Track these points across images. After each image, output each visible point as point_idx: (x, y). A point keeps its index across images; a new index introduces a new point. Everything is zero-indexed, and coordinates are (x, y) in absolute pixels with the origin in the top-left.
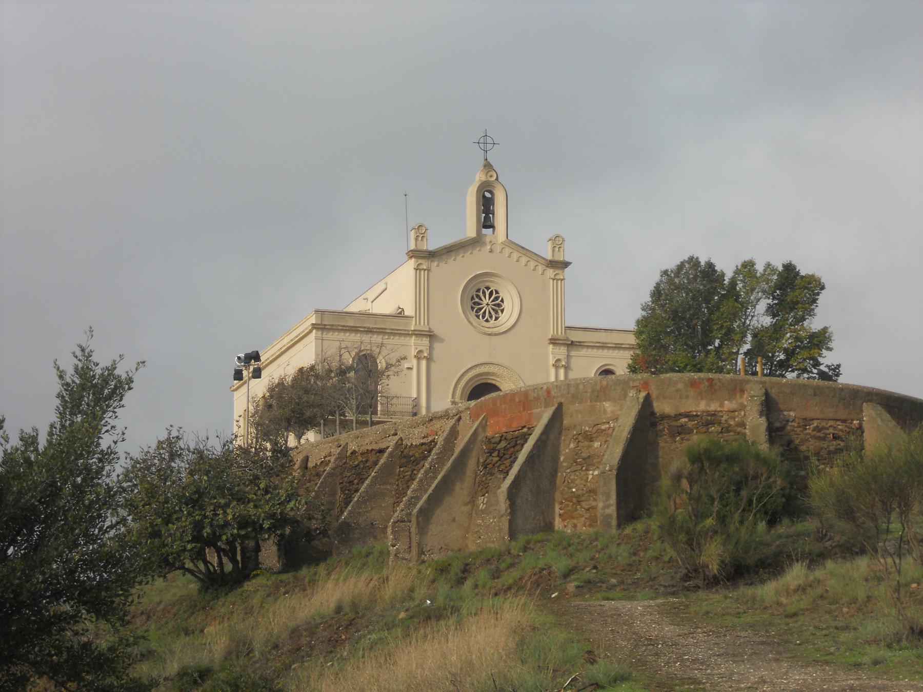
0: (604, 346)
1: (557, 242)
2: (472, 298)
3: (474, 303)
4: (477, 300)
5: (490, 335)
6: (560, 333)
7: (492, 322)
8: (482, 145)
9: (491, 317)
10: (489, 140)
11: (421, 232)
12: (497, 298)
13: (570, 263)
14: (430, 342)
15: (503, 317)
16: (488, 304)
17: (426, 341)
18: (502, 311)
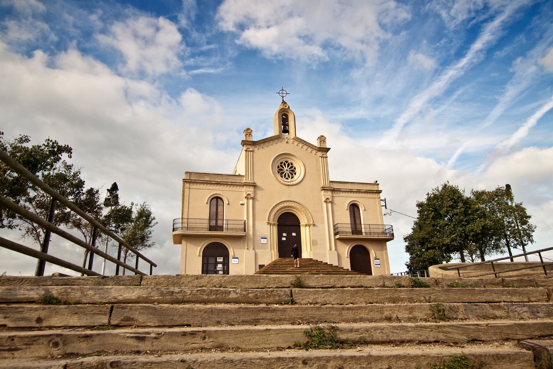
0: (351, 191)
1: (322, 139)
2: (278, 167)
3: (280, 170)
4: (281, 168)
5: (289, 185)
6: (327, 185)
7: (290, 179)
8: (281, 94)
9: (289, 177)
11: (248, 132)
12: (292, 167)
13: (329, 149)
14: (254, 189)
15: (296, 177)
17: (252, 189)
18: (295, 174)
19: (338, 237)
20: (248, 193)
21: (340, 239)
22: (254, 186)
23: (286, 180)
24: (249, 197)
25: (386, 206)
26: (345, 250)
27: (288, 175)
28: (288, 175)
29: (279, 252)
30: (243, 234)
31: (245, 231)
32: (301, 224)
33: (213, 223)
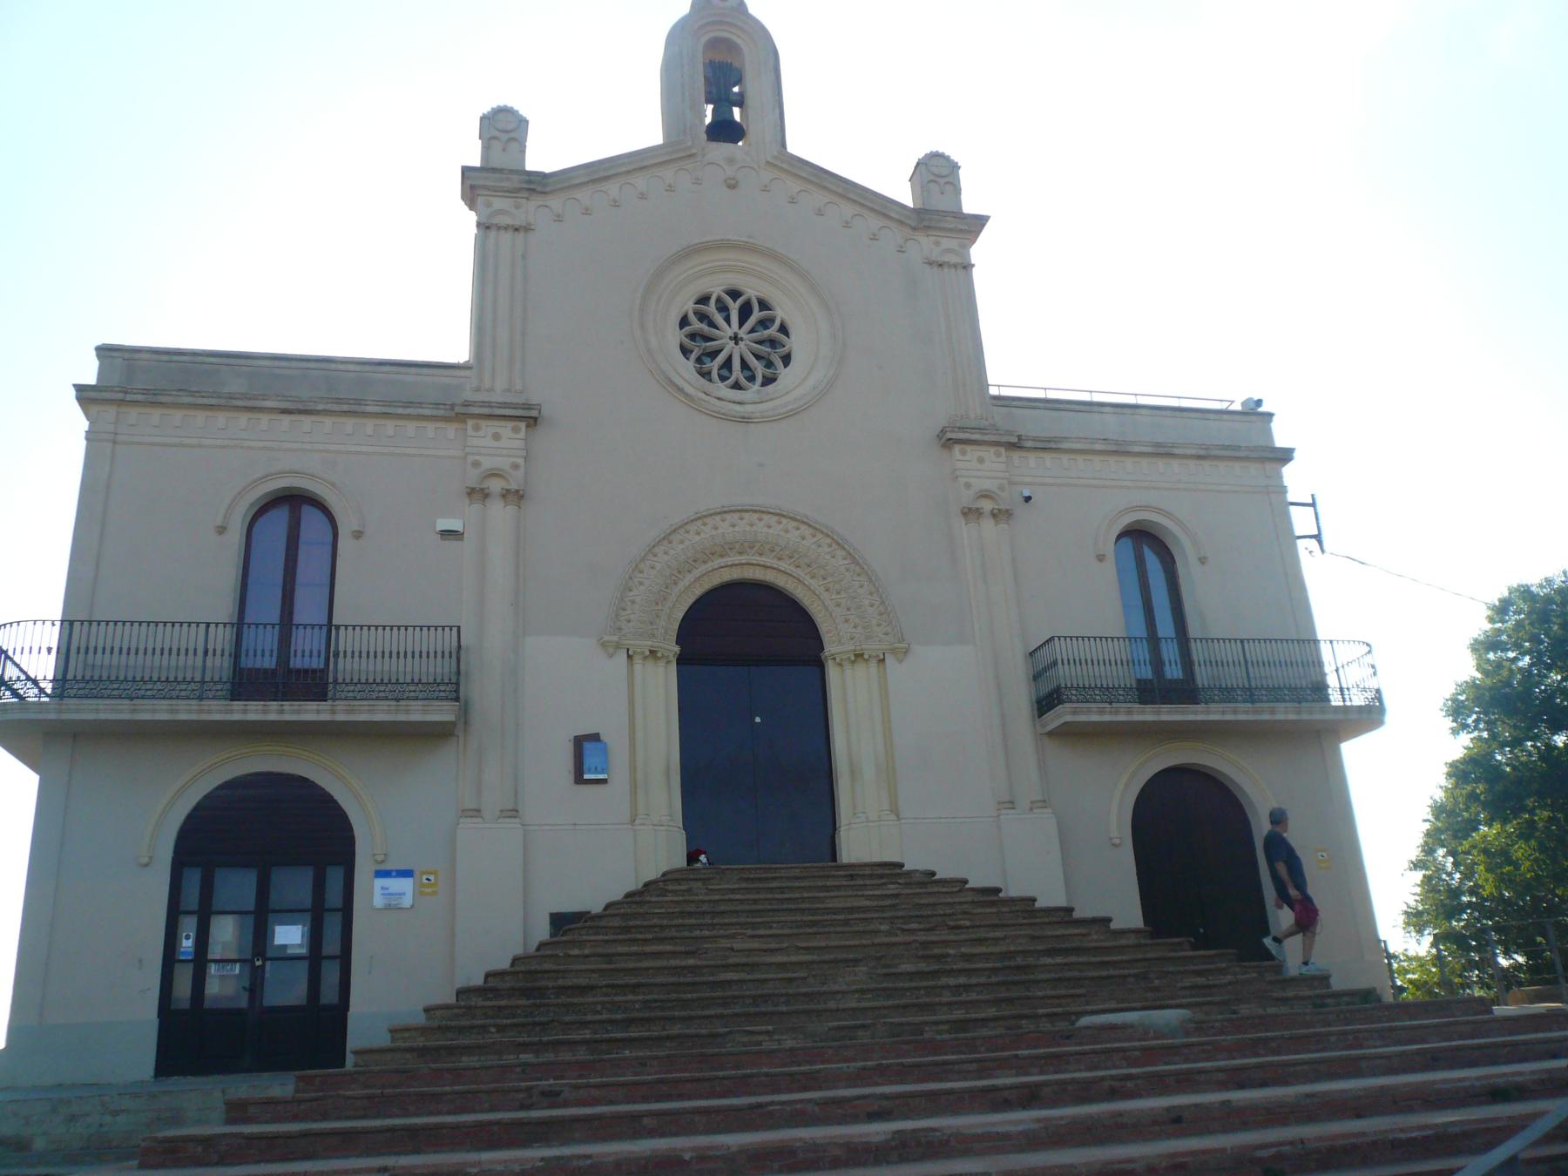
2: (684, 322)
4: (696, 325)
5: (745, 420)
9: (752, 379)
11: (503, 129)
12: (764, 323)
13: (979, 222)
15: (787, 377)
17: (511, 437)
18: (786, 360)
19: (1063, 715)
20: (487, 463)
21: (1070, 734)
22: (530, 419)
24: (495, 486)
25: (1318, 537)
26: (1111, 790)
27: (745, 365)
28: (745, 365)
30: (442, 713)
32: (830, 648)
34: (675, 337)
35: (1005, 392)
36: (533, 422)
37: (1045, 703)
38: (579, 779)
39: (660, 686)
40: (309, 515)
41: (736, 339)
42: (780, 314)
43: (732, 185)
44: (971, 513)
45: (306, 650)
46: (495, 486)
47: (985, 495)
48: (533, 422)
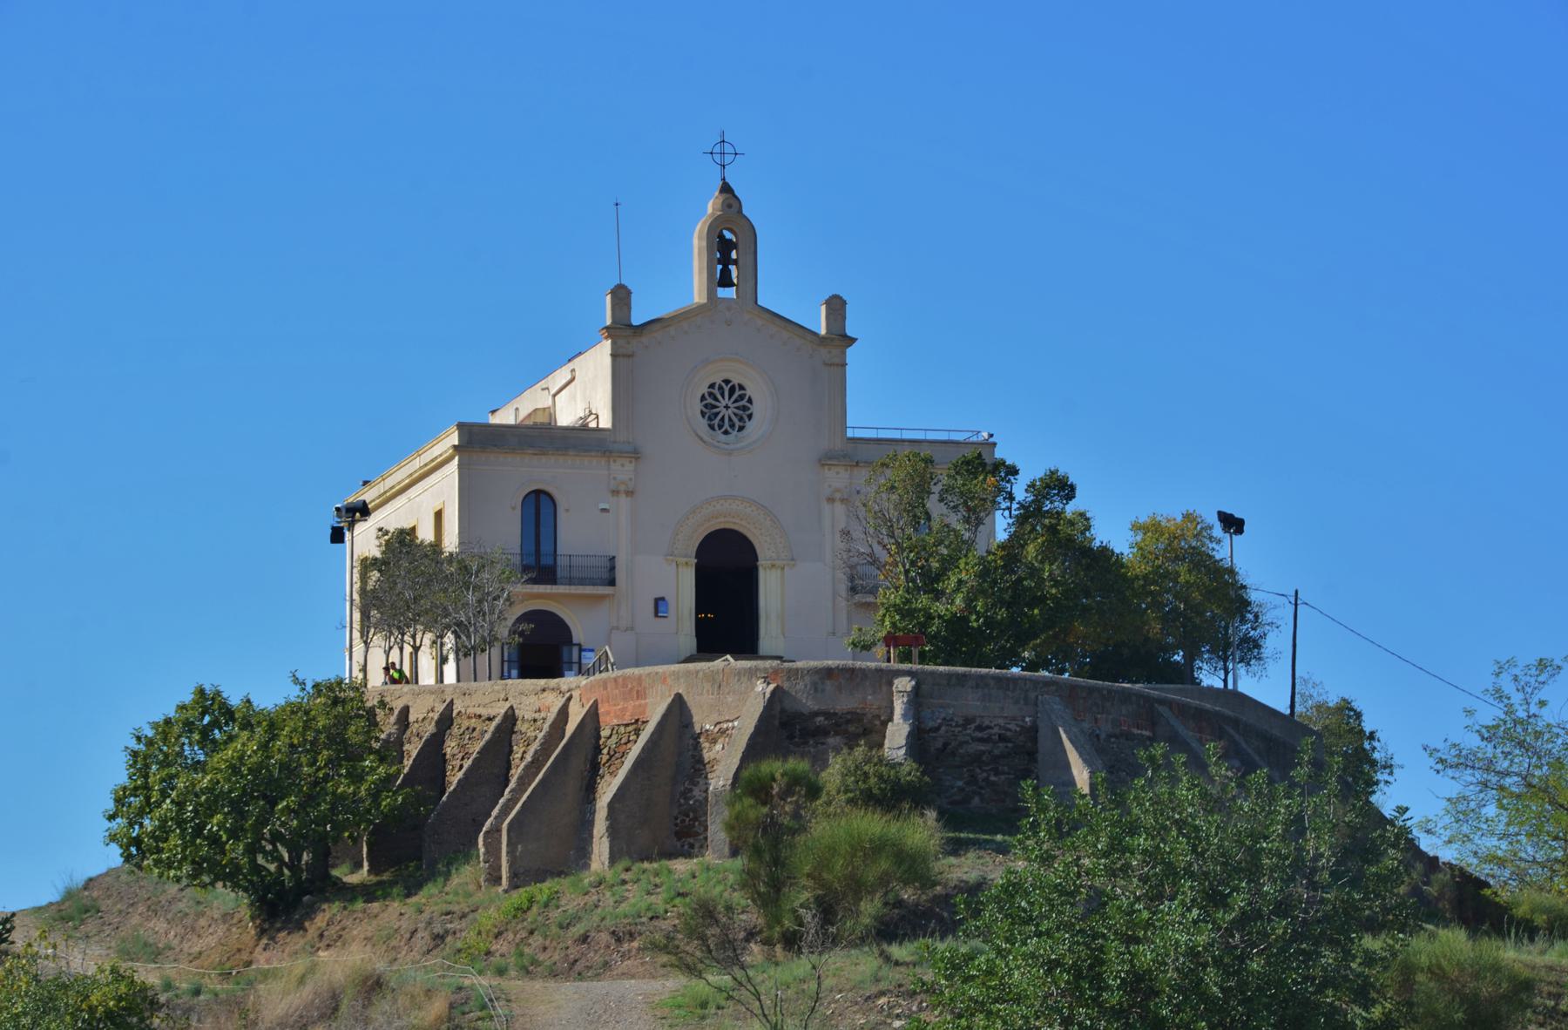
1: (836, 306)
2: (703, 398)
4: (710, 400)
8: (717, 158)
10: (728, 149)
11: (621, 296)
12: (741, 397)
13: (852, 340)
16: (727, 407)
17: (630, 467)
18: (750, 417)
23: (723, 437)
29: (697, 635)
31: (612, 582)
32: (761, 562)
33: (531, 560)
34: (699, 406)
35: (859, 434)
36: (637, 459)
37: (853, 590)
38: (656, 615)
39: (688, 579)
40: (543, 497)
41: (727, 407)
42: (748, 393)
43: (729, 323)
44: (831, 500)
45: (546, 561)
46: (622, 488)
47: (838, 490)
48: (637, 459)
